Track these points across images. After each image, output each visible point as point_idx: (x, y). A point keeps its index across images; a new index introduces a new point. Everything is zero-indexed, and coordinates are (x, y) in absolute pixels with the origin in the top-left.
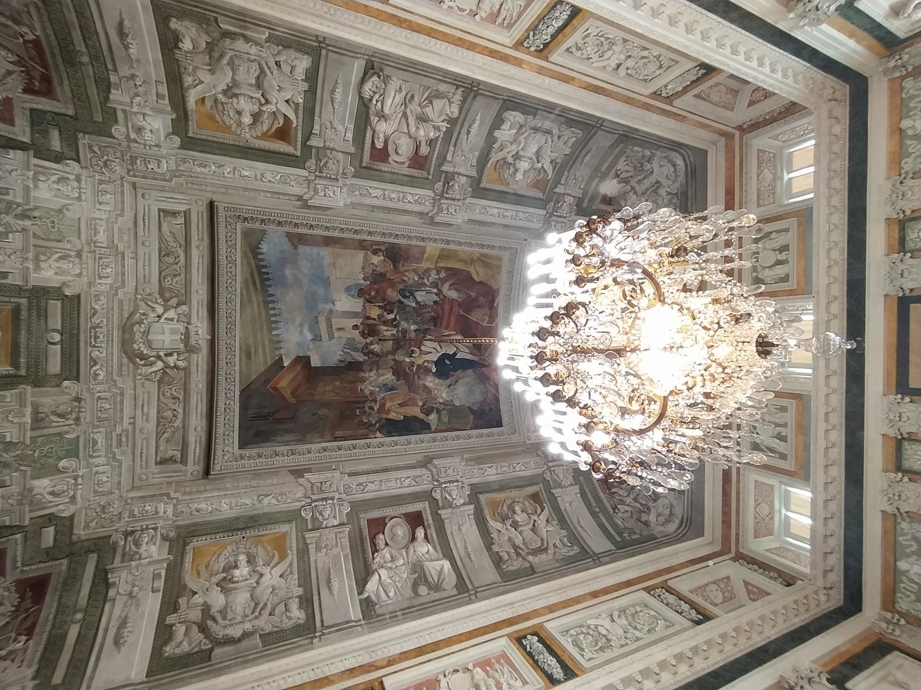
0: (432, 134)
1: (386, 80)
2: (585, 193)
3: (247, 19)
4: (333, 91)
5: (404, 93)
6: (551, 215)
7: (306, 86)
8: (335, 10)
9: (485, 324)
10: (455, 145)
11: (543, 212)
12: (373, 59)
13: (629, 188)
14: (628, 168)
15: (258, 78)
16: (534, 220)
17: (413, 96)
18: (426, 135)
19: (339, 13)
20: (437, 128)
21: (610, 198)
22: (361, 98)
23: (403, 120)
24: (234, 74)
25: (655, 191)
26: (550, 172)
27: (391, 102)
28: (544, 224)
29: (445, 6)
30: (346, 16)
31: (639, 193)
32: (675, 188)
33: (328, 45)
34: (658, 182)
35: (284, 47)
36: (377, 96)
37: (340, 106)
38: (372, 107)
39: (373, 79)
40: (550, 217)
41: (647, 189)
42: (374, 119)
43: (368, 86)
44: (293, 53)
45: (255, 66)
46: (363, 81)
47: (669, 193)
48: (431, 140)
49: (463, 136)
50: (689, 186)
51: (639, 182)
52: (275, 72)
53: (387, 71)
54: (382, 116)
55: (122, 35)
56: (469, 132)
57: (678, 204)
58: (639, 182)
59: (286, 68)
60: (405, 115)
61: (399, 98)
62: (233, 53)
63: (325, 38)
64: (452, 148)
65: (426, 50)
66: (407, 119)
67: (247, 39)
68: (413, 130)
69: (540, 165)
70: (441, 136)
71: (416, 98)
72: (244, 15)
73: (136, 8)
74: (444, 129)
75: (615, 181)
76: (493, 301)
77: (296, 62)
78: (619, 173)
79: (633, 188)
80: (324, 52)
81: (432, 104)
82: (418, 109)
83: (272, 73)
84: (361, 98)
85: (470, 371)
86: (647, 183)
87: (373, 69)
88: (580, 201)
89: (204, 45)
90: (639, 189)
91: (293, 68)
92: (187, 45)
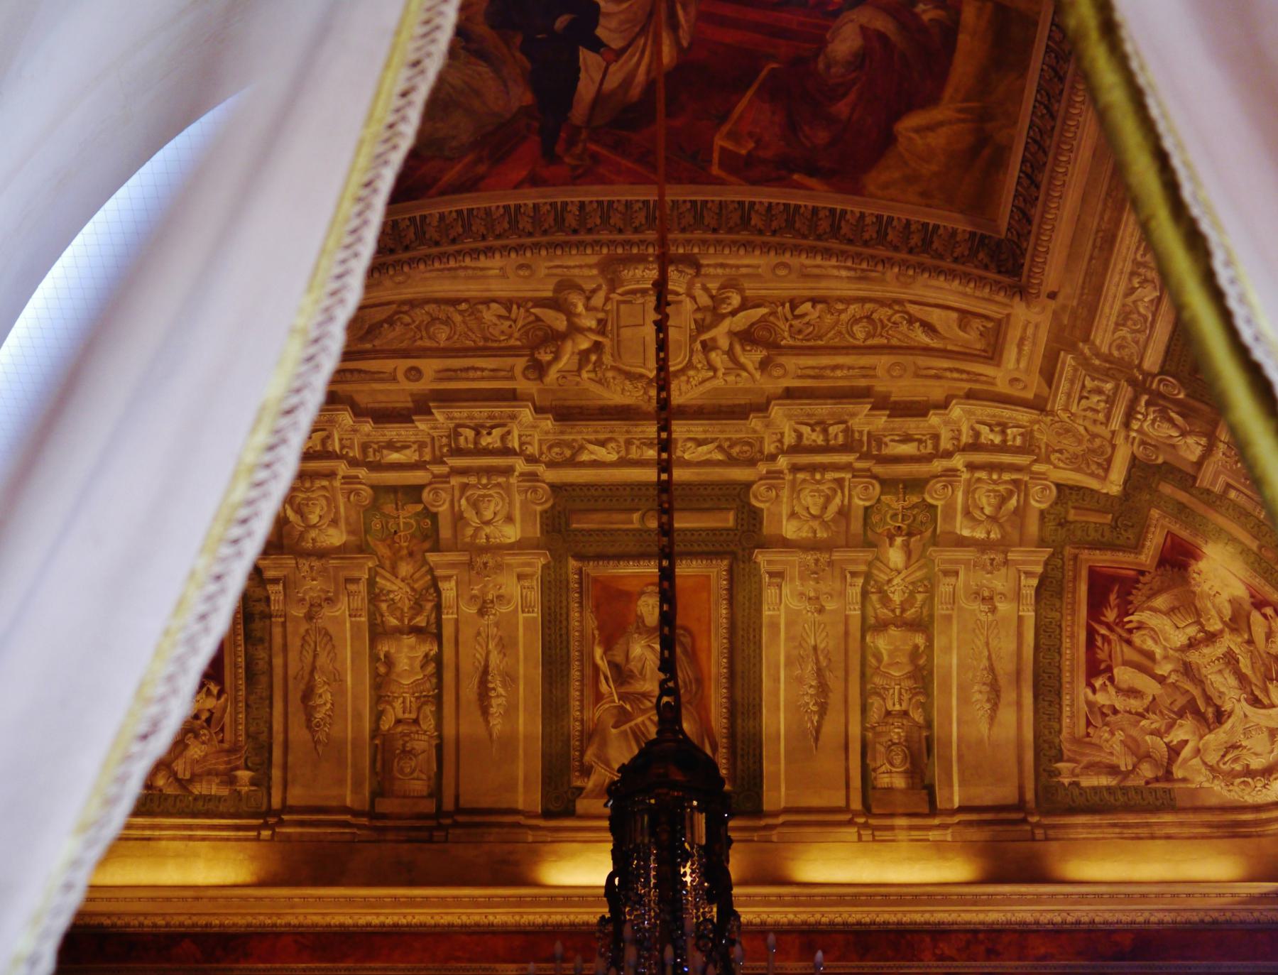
2: (1214, 500)
6: (1139, 387)
9: (719, 142)
11: (1152, 361)
13: (1215, 625)
16: (1124, 332)
21: (1184, 567)
25: (1190, 709)
28: (1107, 358)
31: (1193, 657)
32: (1193, 774)
34: (1220, 716)
40: (1132, 382)
41: (1200, 682)
47: (1174, 751)
50: (1191, 818)
51: (1230, 659)
57: (1129, 783)
58: (1230, 659)
75: (1240, 591)
76: (812, 170)
79: (1211, 638)
85: (528, 98)
86: (1224, 685)
88: (1186, 478)
90: (1205, 657)
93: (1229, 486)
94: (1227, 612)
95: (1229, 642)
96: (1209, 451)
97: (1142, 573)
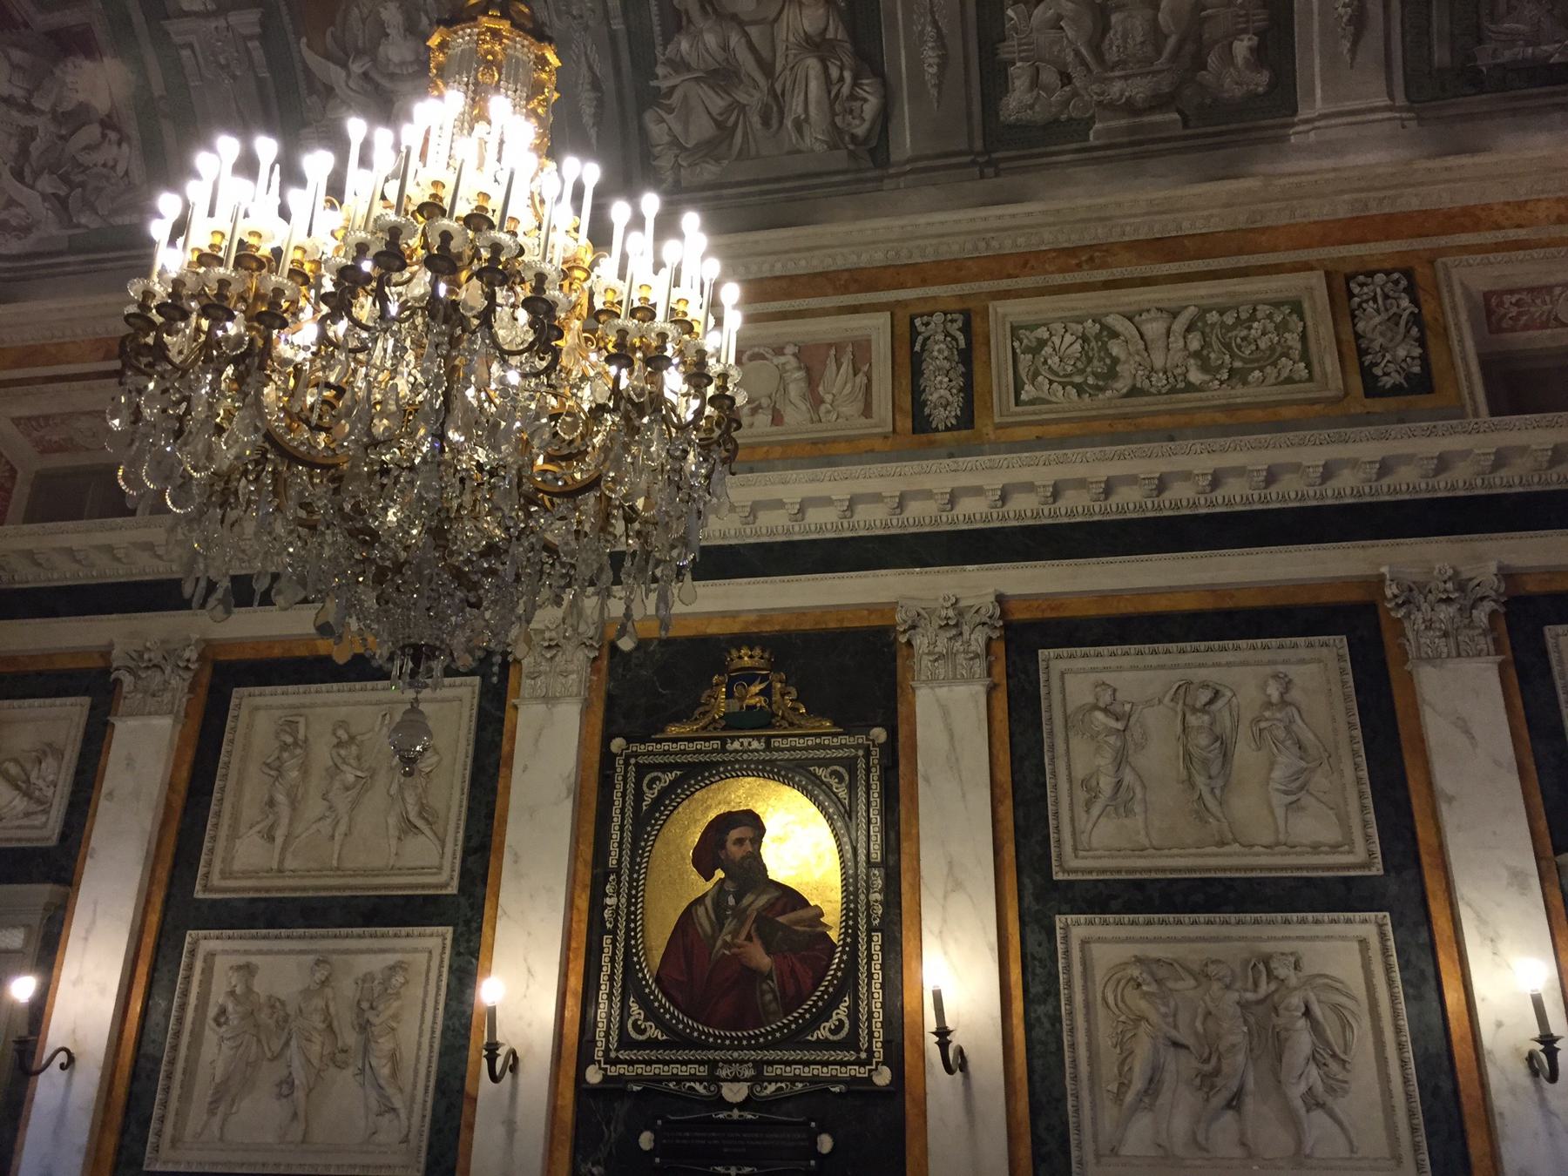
0: (685, 45)
1: (837, 136)
3: (1129, 150)
4: (943, 64)
5: (789, 123)
7: (1007, 50)
8: (976, 249)
10: (613, 36)
12: (877, 173)
13: (43, 104)
14: (99, 157)
15: (1106, 28)
17: (766, 122)
18: (696, 37)
19: (969, 246)
20: (679, 65)
22: (878, 73)
23: (765, 53)
24: (1155, 19)
26: (313, 60)
27: (809, 88)
29: (790, 350)
30: (956, 247)
33: (973, 163)
35: (1056, 121)
36: (845, 90)
37: (922, 33)
38: (847, 60)
39: (866, 125)
42: (836, 31)
43: (871, 106)
44: (1039, 115)
45: (1112, 56)
46: (885, 115)
48: (679, 28)
49: (603, 69)
52: (1070, 58)
53: (840, 159)
54: (818, 45)
55: (1359, 21)
56: (596, 85)
59: (1049, 76)
60: (767, 68)
61: (796, 107)
62: (1158, 65)
63: (982, 176)
64: (618, 25)
65: (786, 252)
66: (760, 61)
67: (1130, 108)
68: (735, 39)
69: (356, 68)
70: (659, 49)
71: (756, 120)
72: (1135, 157)
73: (1323, 81)
74: (660, 70)
75: (101, 104)
77: (1028, 98)
78: (113, 136)
79: (28, 109)
80: (979, 145)
81: (719, 125)
82: (742, 98)
83: (1077, 53)
84: (878, 73)
87: (872, 152)
89: (1212, 60)
91: (1035, 83)
92: (1242, 47)
93: (191, 46)
94: (67, 106)
95: (42, 124)
96: (206, 15)
97: (26, 25)
